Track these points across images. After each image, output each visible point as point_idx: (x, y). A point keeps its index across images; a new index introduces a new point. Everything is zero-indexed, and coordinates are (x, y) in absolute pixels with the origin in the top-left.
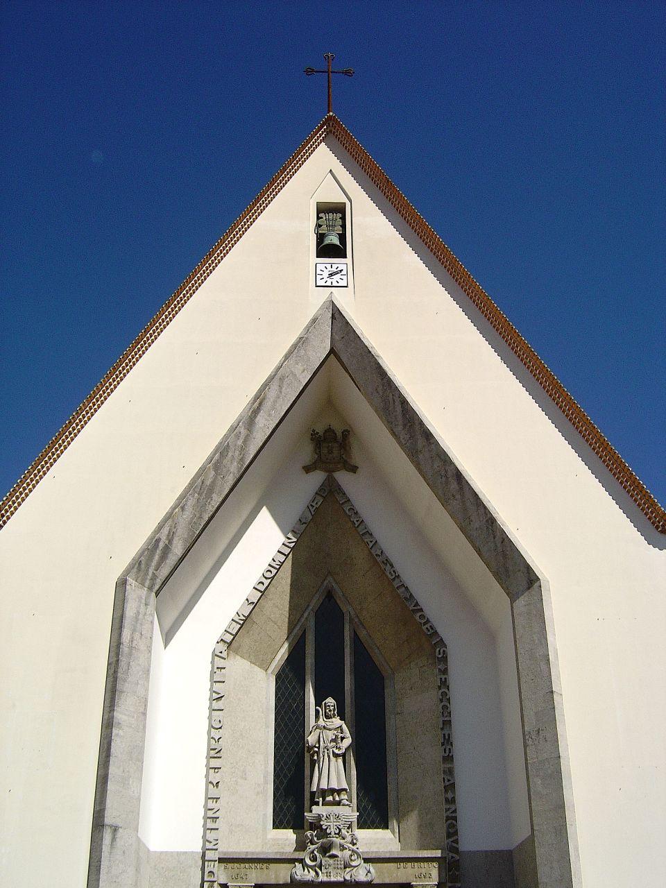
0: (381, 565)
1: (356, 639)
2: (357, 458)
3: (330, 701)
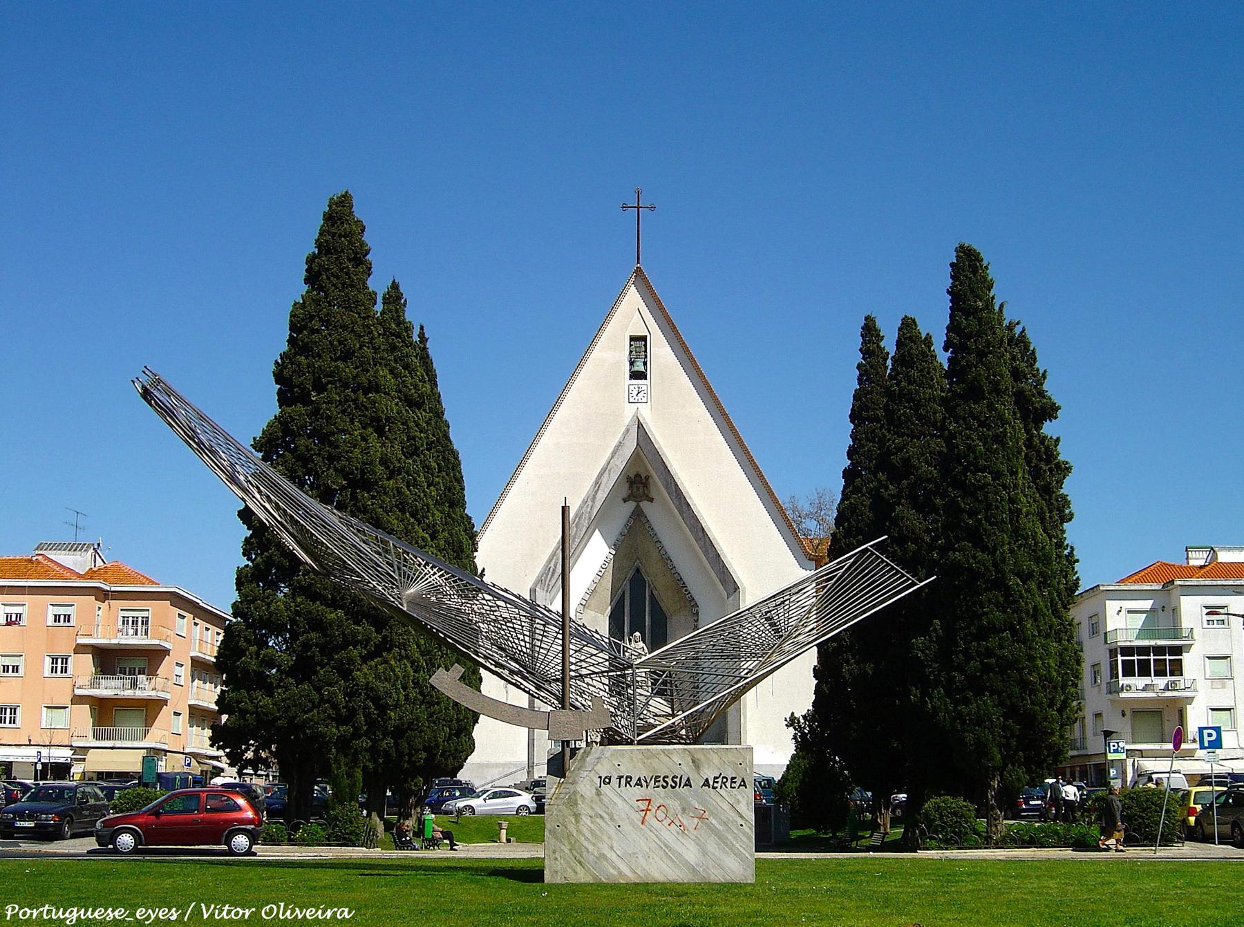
0: (666, 559)
1: (652, 595)
2: (653, 494)
3: (638, 634)
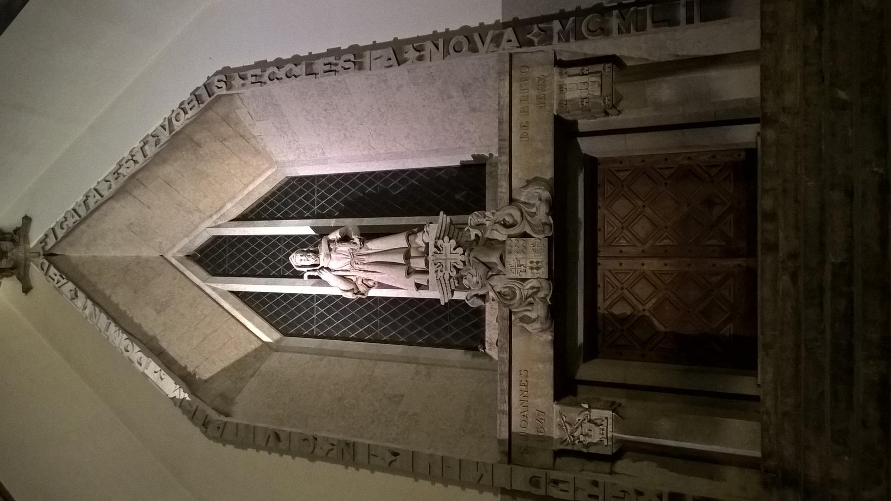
1: (244, 218)
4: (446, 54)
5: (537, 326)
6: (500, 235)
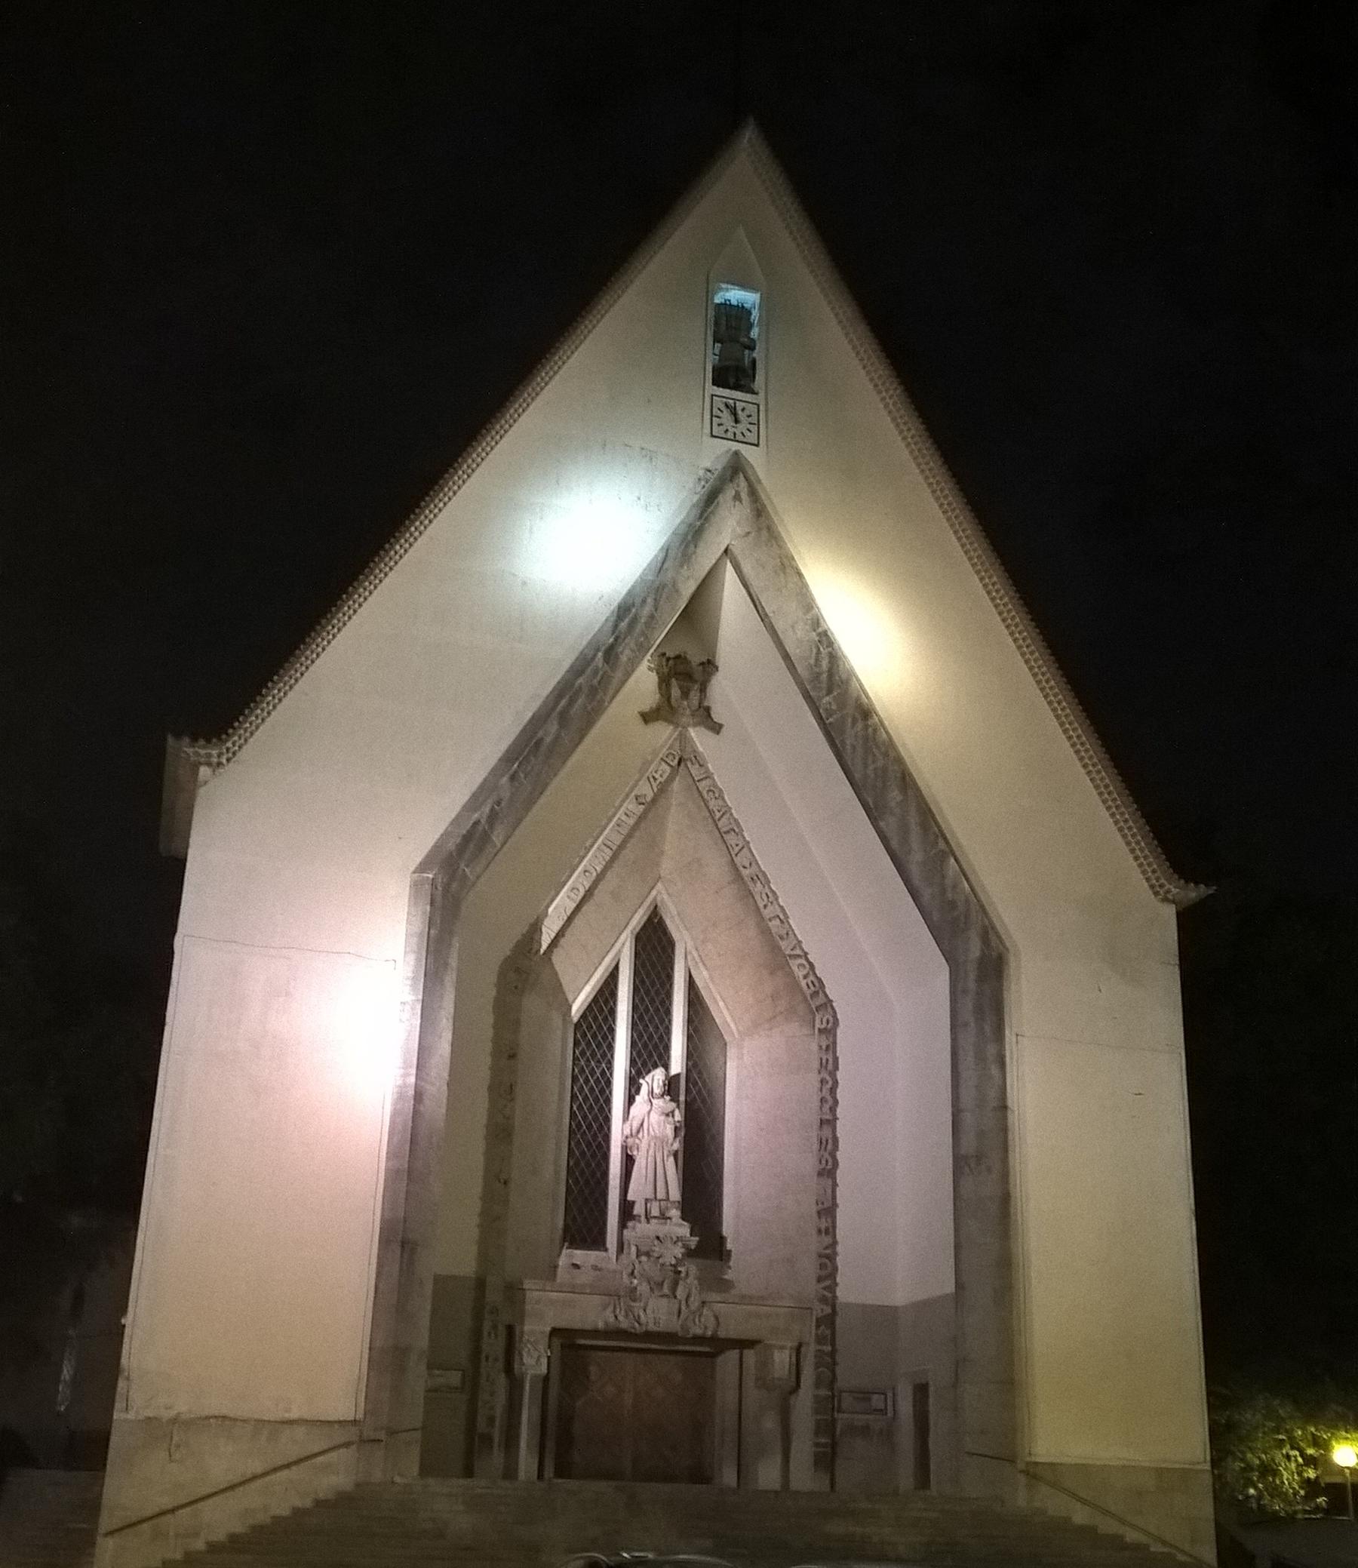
4: (820, 1256)
5: (612, 1319)
6: (680, 1292)
